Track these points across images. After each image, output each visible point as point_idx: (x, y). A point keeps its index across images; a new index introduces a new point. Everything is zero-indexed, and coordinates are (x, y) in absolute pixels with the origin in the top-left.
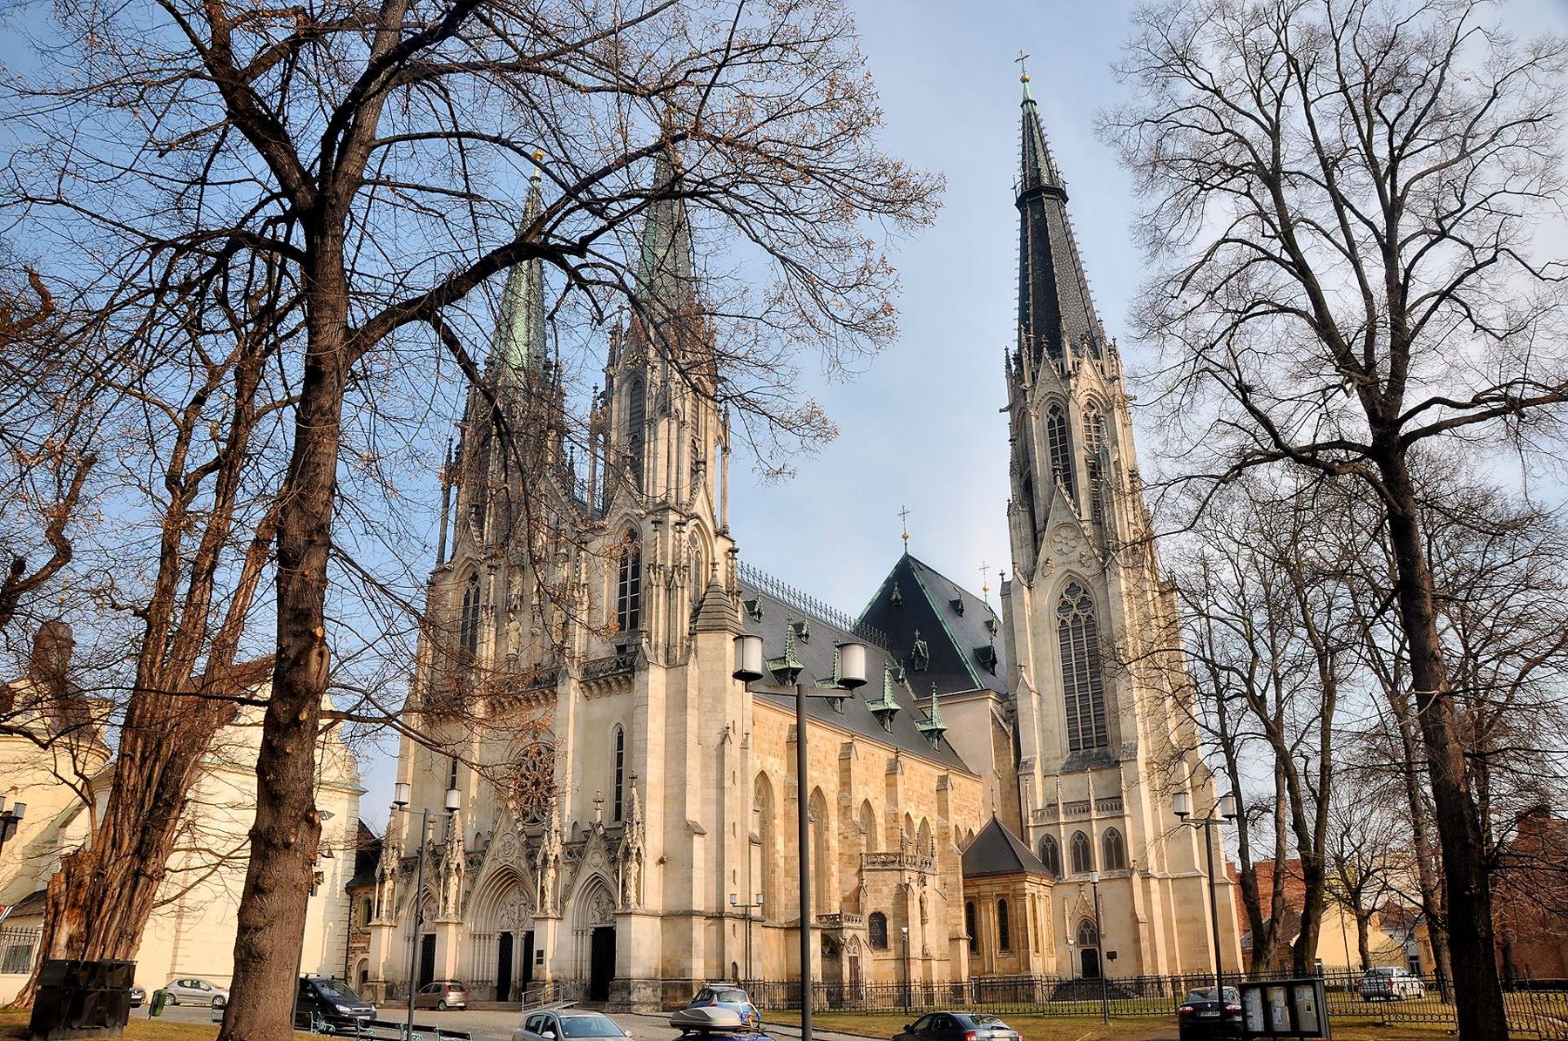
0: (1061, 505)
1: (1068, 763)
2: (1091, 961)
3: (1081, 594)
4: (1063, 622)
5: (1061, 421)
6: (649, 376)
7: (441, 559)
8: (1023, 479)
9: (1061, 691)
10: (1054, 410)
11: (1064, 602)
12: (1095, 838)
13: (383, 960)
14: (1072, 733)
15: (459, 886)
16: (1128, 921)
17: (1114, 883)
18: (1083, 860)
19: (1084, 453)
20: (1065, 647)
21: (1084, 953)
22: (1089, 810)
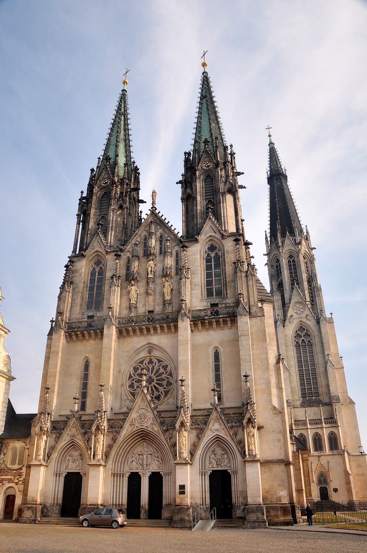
0: (296, 294)
1: (302, 402)
2: (324, 493)
3: (305, 331)
4: (297, 342)
5: (294, 261)
6: (220, 173)
7: (74, 251)
8: (278, 282)
9: (297, 371)
10: (291, 256)
11: (298, 334)
12: (325, 436)
13: (40, 489)
14: (303, 390)
15: (103, 441)
16: (343, 474)
17: (335, 456)
18: (318, 445)
19: (306, 275)
20: (298, 353)
21: (321, 489)
22: (321, 423)
